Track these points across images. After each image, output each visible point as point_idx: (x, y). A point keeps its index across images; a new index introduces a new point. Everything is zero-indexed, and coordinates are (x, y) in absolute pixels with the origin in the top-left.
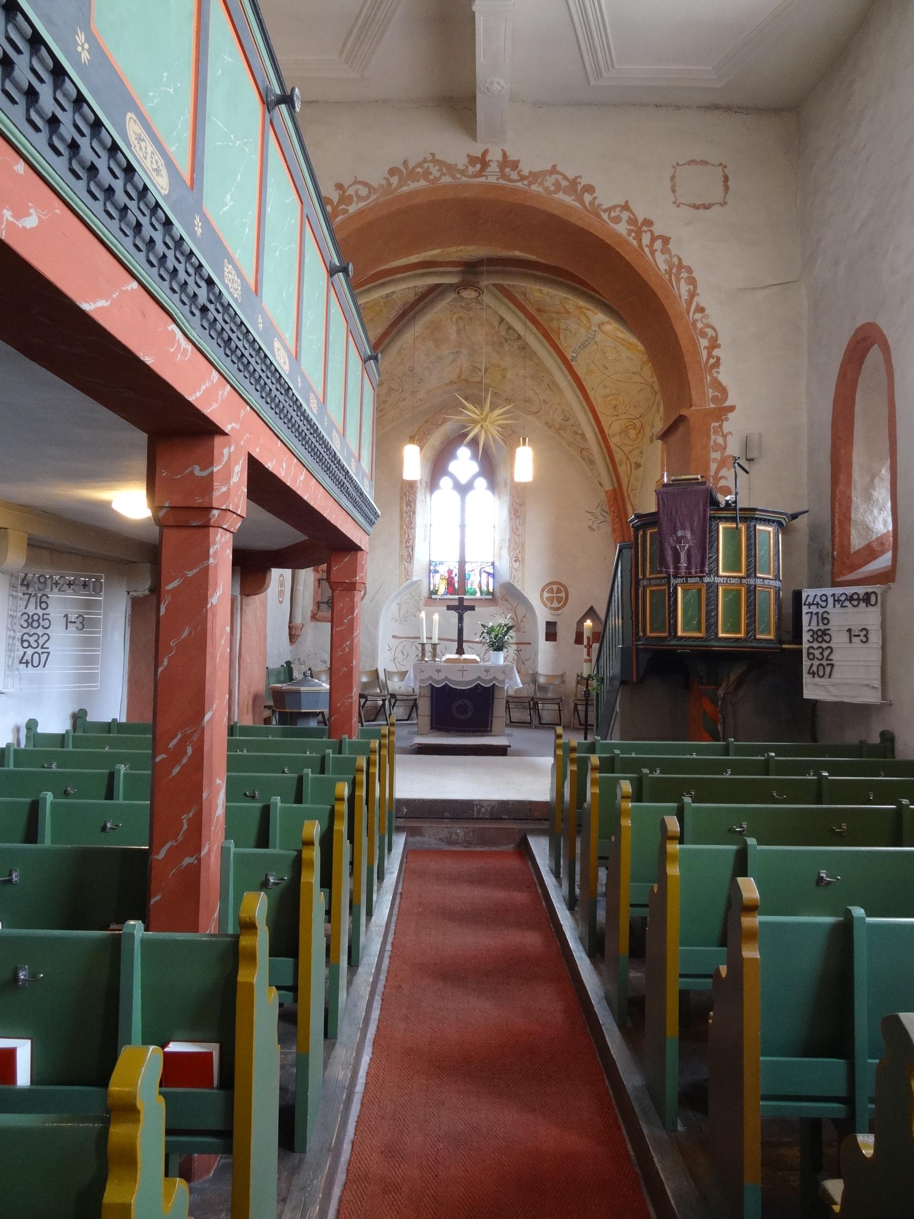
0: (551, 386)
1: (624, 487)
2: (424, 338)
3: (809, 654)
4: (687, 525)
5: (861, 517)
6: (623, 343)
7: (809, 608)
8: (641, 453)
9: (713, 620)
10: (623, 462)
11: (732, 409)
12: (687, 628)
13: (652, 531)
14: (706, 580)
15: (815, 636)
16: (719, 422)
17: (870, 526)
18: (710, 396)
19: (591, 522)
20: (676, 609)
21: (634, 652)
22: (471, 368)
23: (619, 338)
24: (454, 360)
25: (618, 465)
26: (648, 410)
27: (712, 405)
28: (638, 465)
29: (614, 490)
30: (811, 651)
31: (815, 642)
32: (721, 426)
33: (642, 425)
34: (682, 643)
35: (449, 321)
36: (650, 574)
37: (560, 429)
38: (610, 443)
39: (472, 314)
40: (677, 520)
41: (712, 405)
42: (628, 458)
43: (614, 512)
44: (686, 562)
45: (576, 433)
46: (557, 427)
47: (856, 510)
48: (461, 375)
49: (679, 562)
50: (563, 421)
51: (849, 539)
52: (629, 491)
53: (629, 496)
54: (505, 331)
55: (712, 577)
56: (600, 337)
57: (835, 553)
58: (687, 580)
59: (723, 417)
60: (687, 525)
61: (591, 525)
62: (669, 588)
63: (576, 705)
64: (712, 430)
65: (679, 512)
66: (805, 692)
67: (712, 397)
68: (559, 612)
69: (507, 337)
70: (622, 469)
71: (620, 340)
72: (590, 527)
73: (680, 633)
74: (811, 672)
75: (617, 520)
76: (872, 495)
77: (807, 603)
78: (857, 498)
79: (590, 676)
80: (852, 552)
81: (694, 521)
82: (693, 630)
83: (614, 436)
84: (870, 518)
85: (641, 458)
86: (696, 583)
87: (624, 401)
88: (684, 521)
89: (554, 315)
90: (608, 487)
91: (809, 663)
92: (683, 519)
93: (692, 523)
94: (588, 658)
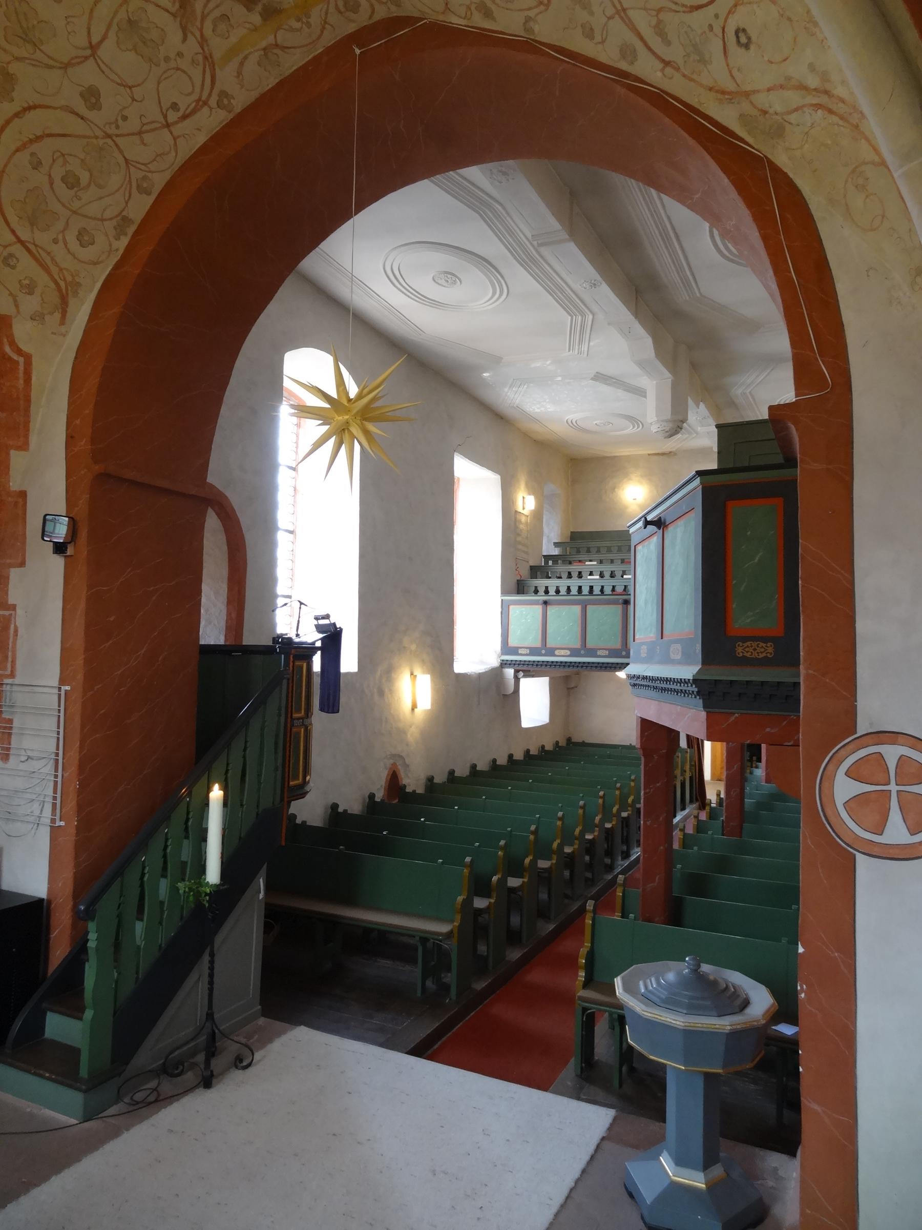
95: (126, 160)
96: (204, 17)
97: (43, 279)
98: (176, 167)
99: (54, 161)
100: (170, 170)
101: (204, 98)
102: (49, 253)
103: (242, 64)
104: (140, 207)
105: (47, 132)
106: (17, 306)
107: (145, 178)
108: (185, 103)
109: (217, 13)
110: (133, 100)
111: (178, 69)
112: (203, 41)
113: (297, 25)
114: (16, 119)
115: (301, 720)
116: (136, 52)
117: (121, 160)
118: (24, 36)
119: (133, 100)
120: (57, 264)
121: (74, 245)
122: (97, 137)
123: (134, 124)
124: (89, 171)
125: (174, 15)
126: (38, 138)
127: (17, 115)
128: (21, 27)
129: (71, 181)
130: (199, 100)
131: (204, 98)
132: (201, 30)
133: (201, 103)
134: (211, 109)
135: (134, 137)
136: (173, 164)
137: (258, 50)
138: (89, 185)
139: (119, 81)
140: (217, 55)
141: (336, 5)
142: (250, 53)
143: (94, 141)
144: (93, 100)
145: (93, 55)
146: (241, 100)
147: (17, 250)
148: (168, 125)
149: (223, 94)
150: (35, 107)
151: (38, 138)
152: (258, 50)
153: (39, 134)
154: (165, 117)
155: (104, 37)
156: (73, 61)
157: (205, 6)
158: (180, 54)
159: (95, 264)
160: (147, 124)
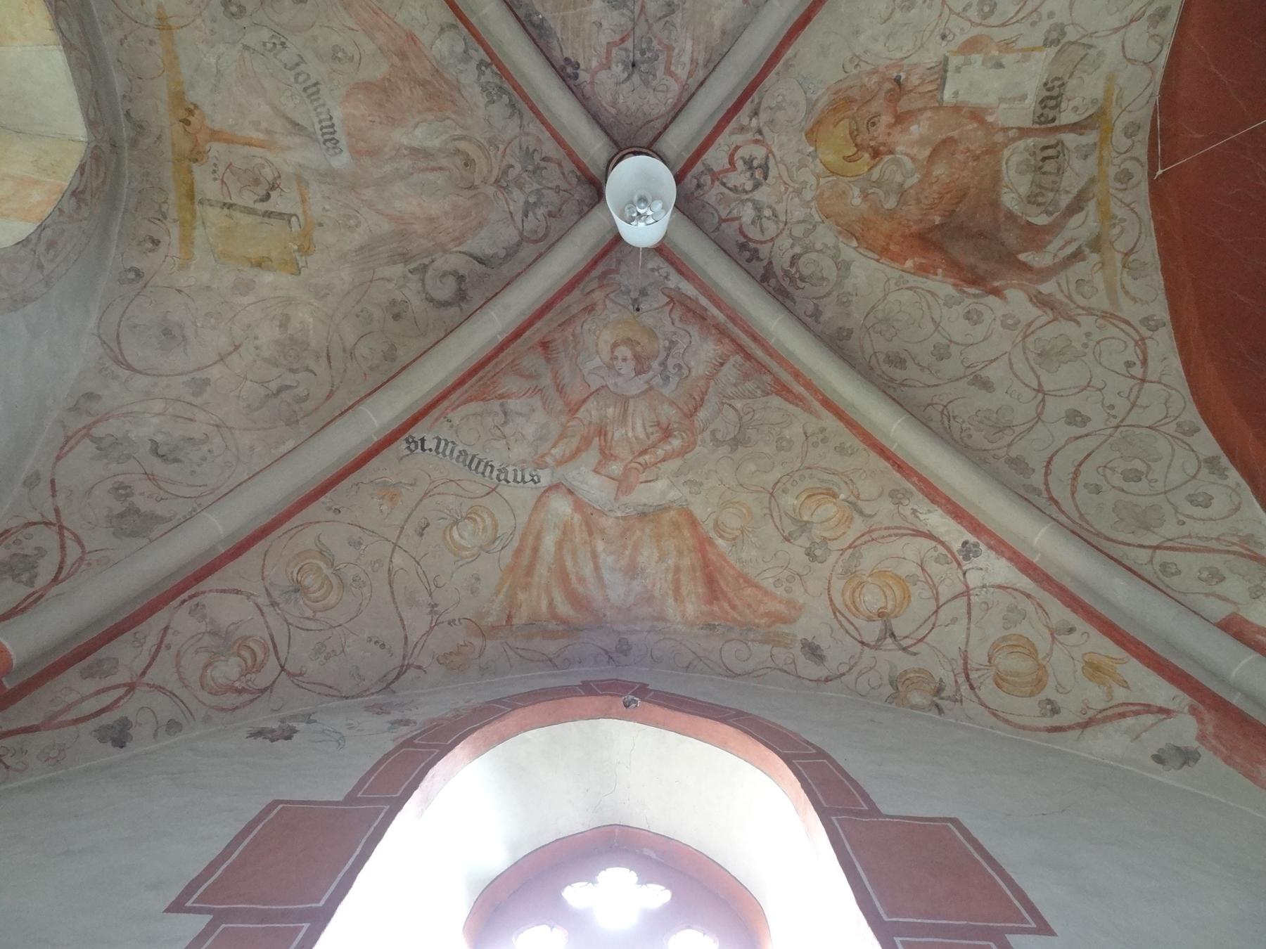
0: (284, 395)
2: (403, 56)
6: (528, 552)
8: (173, 726)
22: (268, 173)
23: (538, 537)
24: (296, 127)
35: (459, 132)
39: (491, 190)
42: (131, 687)
46: (99, 431)
48: (230, 140)
50: (149, 446)
54: (447, 268)
56: (523, 495)
69: (430, 272)
85: (155, 735)
87: (326, 609)
89: (547, 381)
95: (1149, 427)
96: (1070, 297)
97: (1215, 560)
98: (1189, 397)
99: (1104, 476)
100: (1188, 403)
101: (1138, 338)
102: (1190, 536)
103: (1127, 293)
104: (1206, 443)
105: (1076, 463)
106: (1225, 599)
107: (1179, 425)
108: (1132, 354)
109: (1073, 287)
110: (1100, 390)
111: (1098, 343)
112: (1089, 311)
113: (1116, 230)
114: (1049, 477)
116: (1064, 363)
117: (1145, 431)
118: (998, 430)
119: (1100, 390)
120: (1208, 539)
121: (1198, 512)
122: (1111, 436)
123: (1122, 405)
124: (1135, 458)
125: (1055, 319)
126: (1076, 474)
127: (1046, 474)
128: (992, 426)
129: (1136, 476)
130: (1136, 343)
131: (1138, 338)
132: (1078, 306)
133: (1141, 342)
134: (1150, 338)
135: (1133, 412)
136: (1184, 398)
137: (1122, 273)
138: (1149, 466)
139: (1077, 390)
140: (1106, 306)
141: (1117, 189)
142: (1121, 279)
143: (1111, 439)
144: (1079, 419)
145: (1045, 394)
146: (1160, 309)
147: (1161, 556)
148: (1143, 380)
149: (1145, 321)
150: (1051, 458)
151: (1076, 474)
152: (1122, 273)
153: (1073, 469)
154: (1133, 377)
155: (1038, 377)
156: (1039, 410)
157: (1062, 291)
158: (1088, 335)
159: (1237, 509)
160: (1129, 396)
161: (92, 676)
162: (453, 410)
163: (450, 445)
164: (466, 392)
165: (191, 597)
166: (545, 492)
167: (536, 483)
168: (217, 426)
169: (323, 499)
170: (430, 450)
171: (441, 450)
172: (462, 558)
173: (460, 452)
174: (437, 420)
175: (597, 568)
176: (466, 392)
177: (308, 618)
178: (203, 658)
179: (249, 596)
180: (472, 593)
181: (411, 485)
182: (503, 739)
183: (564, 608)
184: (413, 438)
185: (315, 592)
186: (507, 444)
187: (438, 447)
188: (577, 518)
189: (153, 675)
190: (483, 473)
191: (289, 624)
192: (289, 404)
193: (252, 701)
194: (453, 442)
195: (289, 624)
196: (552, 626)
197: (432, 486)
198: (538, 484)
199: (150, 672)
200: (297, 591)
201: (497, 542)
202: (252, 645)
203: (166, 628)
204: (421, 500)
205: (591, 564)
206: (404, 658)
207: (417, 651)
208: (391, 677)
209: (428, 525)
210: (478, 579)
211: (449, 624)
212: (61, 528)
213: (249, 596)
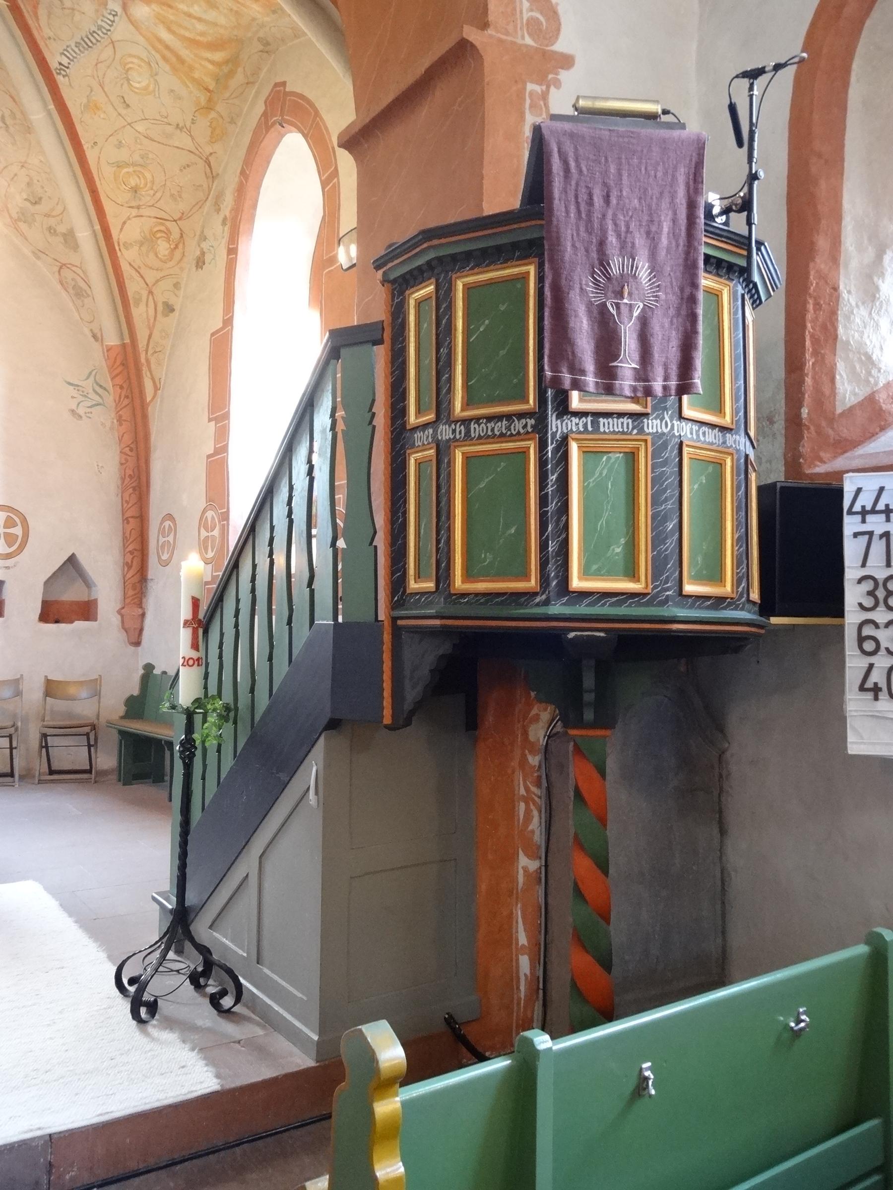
1: (141, 345)
3: (861, 640)
4: (640, 241)
5: (856, 335)
6: (168, 54)
7: (864, 521)
8: (177, 286)
9: (671, 542)
10: (140, 300)
11: (567, 61)
12: (595, 567)
13: (471, 279)
14: (652, 426)
15: (881, 594)
16: (541, 85)
17: (874, 357)
18: (525, 17)
19: (75, 402)
20: (564, 508)
21: (387, 637)
23: (160, 40)
25: (131, 302)
26: (198, 207)
27: (528, 41)
28: (169, 309)
29: (124, 346)
30: (867, 631)
31: (881, 608)
32: (545, 96)
33: (182, 236)
34: (582, 609)
36: (467, 405)
37: (19, 220)
38: (120, 259)
40: (610, 226)
41: (528, 41)
42: (151, 292)
43: (121, 387)
44: (636, 356)
45: (51, 230)
46: (15, 216)
47: (848, 318)
49: (616, 357)
50: (28, 204)
51: (833, 380)
52: (149, 354)
53: (148, 361)
55: (667, 418)
56: (122, 30)
57: (805, 412)
58: (595, 424)
59: (550, 76)
60: (640, 241)
61: (74, 407)
62: (542, 446)
63: (44, 736)
64: (528, 102)
65: (614, 201)
66: (851, 738)
67: (528, 20)
68: (9, 562)
70: (139, 313)
71: (160, 47)
72: (73, 411)
73: (576, 583)
74: (869, 684)
75: (126, 402)
76: (877, 289)
77: (857, 508)
78: (849, 292)
79: (197, 700)
80: (839, 410)
81: (659, 232)
82: (610, 574)
83: (127, 246)
84: (874, 340)
86: (623, 433)
87: (153, 182)
88: (628, 231)
90: (112, 339)
91: (864, 662)
92: (628, 227)
93: (652, 239)
94: (194, 655)
115: (431, 431)
161: (138, 304)
162: (41, 30)
163: (69, 49)
164: (28, 12)
165: (119, 245)
166: (126, 14)
167: (116, 15)
168: (23, 166)
169: (85, 147)
170: (69, 63)
171: (71, 58)
172: (154, 91)
173: (76, 46)
174: (46, 45)
175: (199, 19)
176: (28, 12)
177: (154, 195)
178: (151, 255)
179: (129, 218)
180: (180, 99)
181: (92, 91)
182: (254, 206)
183: (218, 56)
184: (57, 69)
185: (141, 183)
186: (79, 11)
187: (68, 58)
188: (154, 6)
189: (150, 280)
190: (97, 41)
191: (153, 206)
192: (15, 124)
193: (184, 243)
194: (67, 47)
195: (153, 206)
196: (226, 69)
197: (96, 77)
198: (119, 14)
199: (148, 282)
200: (136, 192)
201: (153, 65)
202: (155, 230)
203: (130, 264)
204: (104, 91)
205: (193, 21)
206: (202, 159)
207: (200, 150)
208: (209, 174)
209: (123, 97)
210: (172, 91)
211: (193, 123)
212: (65, 265)
213: (129, 218)
